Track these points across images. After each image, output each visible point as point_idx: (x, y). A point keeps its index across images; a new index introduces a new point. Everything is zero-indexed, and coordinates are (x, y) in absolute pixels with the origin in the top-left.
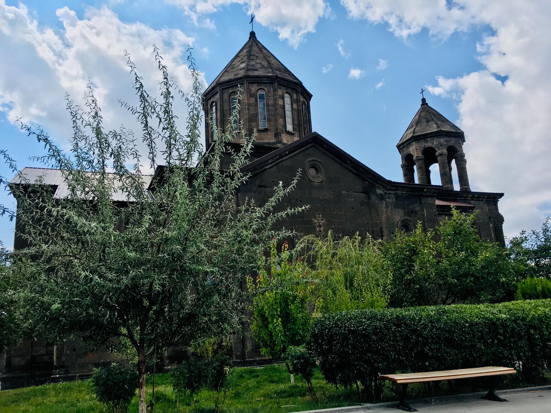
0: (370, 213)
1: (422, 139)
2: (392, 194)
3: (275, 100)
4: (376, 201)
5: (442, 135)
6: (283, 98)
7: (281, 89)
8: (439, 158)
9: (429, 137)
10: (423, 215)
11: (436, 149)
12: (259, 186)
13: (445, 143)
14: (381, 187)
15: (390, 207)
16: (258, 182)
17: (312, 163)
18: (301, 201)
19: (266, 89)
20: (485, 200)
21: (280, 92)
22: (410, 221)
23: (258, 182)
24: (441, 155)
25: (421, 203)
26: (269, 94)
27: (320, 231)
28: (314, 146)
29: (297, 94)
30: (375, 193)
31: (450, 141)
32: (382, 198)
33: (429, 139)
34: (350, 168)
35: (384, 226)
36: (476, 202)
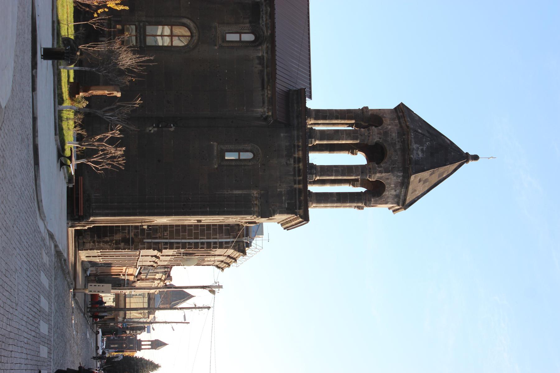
9: (400, 123)
13: (389, 139)
20: (297, 186)
31: (395, 151)
33: (397, 121)
36: (291, 169)
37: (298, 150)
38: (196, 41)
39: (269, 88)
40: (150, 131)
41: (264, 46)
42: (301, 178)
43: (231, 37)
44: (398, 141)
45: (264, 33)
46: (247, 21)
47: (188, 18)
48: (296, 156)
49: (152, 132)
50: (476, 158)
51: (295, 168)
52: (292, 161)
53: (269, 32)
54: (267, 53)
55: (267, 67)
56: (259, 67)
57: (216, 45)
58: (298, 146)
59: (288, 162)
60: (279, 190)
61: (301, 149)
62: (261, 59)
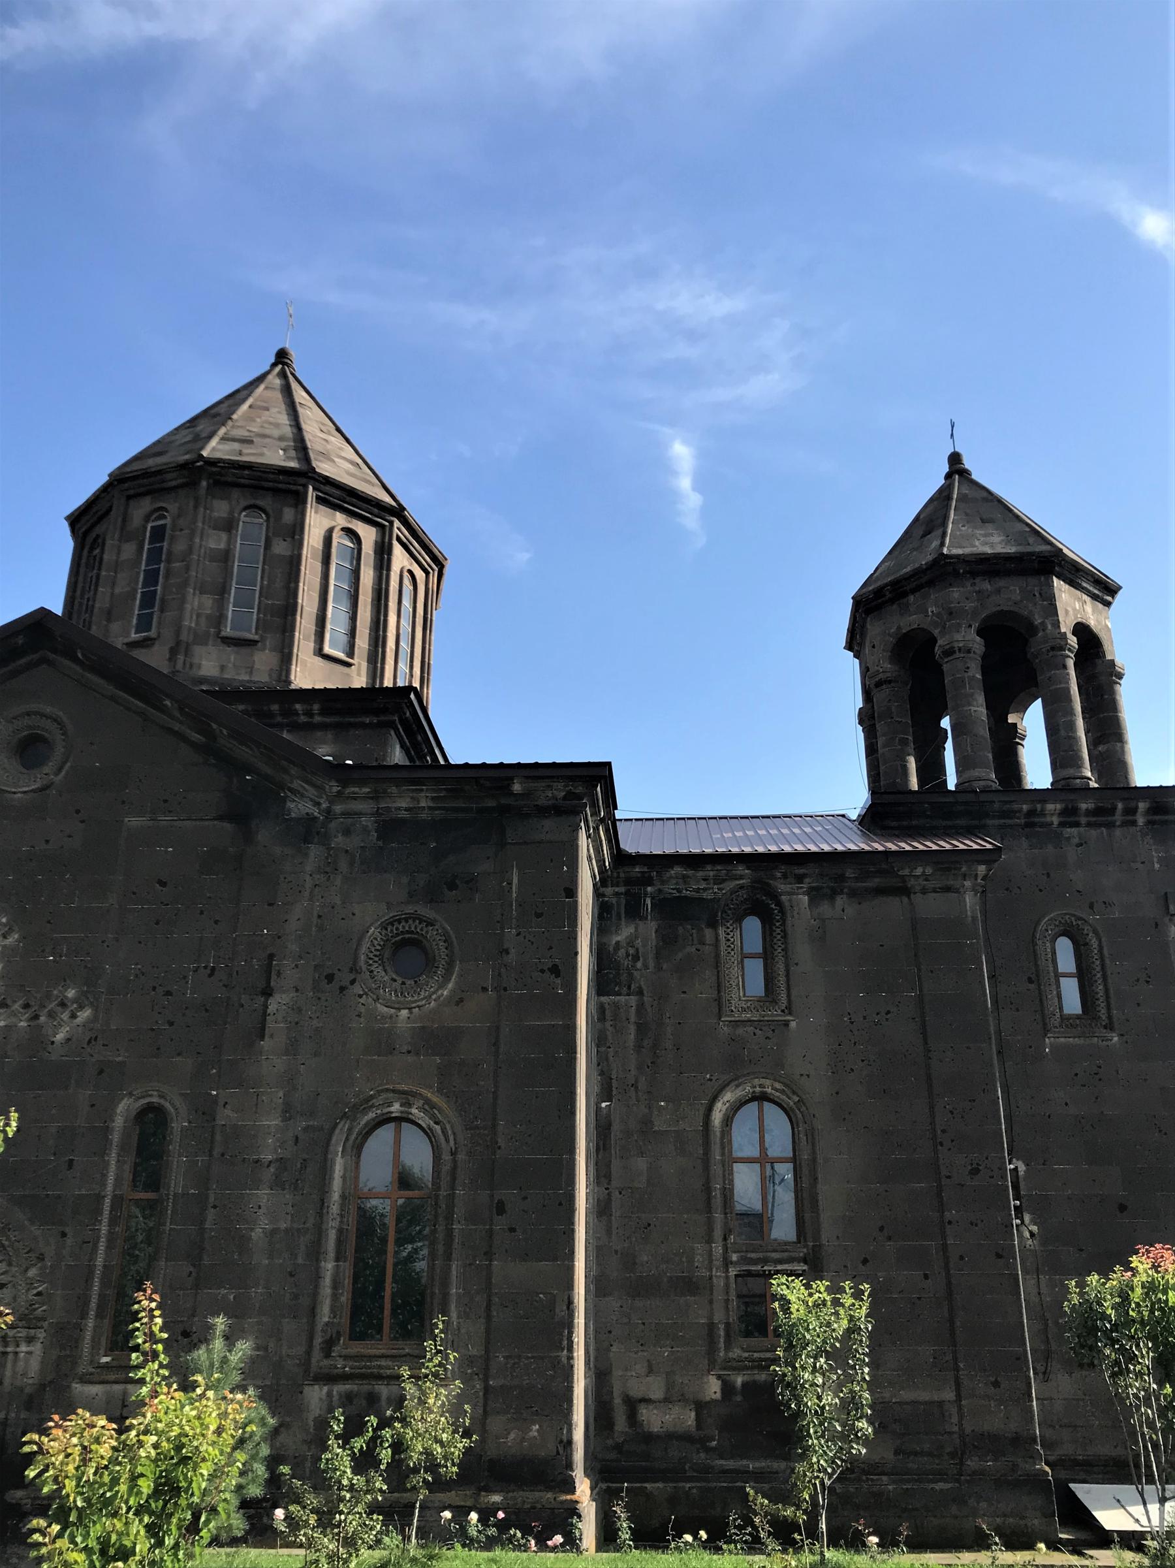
1: (892, 601)
2: (360, 814)
4: (278, 850)
5: (956, 574)
8: (945, 667)
9: (913, 591)
11: (936, 632)
13: (969, 605)
15: (343, 866)
17: (26, 721)
20: (1141, 821)
21: (221, 508)
22: (430, 923)
24: (949, 652)
31: (998, 591)
32: (307, 832)
33: (911, 598)
34: (177, 727)
35: (294, 947)
36: (1094, 833)
37: (1043, 814)
38: (778, 1085)
39: (906, 872)
40: (1032, 1234)
41: (782, 887)
42: (1120, 806)
43: (755, 983)
44: (974, 584)
45: (742, 887)
46: (708, 933)
47: (710, 1109)
48: (1056, 820)
49: (1035, 1228)
50: (955, 458)
51: (1089, 825)
52: (1068, 831)
53: (741, 870)
54: (800, 879)
55: (841, 878)
56: (840, 901)
57: (786, 1024)
58: (1031, 813)
59: (1076, 840)
60: (1157, 866)
61: (1039, 806)
62: (816, 895)
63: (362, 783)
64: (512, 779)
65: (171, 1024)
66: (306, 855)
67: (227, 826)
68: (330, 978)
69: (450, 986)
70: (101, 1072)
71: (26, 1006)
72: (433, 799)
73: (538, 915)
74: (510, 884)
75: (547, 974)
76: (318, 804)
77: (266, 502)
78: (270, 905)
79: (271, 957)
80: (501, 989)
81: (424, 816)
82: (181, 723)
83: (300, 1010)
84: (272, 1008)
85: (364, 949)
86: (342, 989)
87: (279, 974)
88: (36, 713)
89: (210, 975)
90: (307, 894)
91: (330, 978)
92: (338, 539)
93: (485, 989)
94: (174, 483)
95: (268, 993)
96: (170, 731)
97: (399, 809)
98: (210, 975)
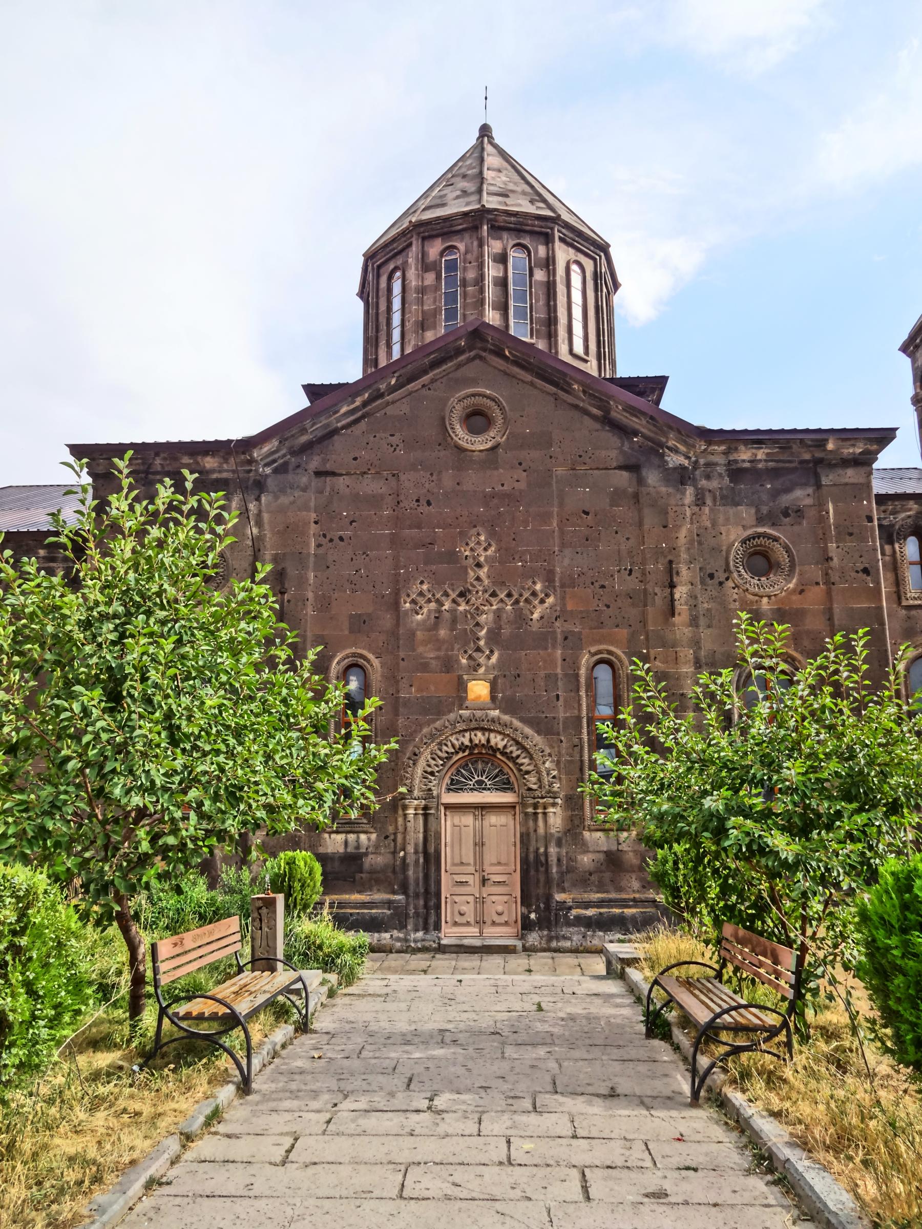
0: (640, 524)
3: (481, 266)
4: (663, 489)
6: (502, 259)
7: (500, 238)
10: (822, 520)
12: (318, 474)
14: (682, 448)
15: (709, 501)
16: (315, 463)
18: (429, 503)
19: (461, 246)
21: (496, 246)
23: (315, 463)
25: (818, 486)
26: (469, 256)
27: (478, 579)
28: (481, 358)
29: (547, 244)
30: (662, 464)
32: (682, 477)
35: (684, 556)
63: (719, 443)
64: (827, 440)
65: (608, 607)
66: (684, 493)
67: (625, 474)
68: (711, 576)
69: (794, 581)
70: (566, 638)
71: (509, 595)
72: (767, 454)
73: (851, 534)
74: (828, 513)
75: (861, 574)
76: (688, 458)
77: (526, 241)
78: (665, 527)
79: (671, 562)
80: (829, 583)
81: (760, 466)
82: (583, 401)
83: (696, 598)
84: (677, 596)
85: (732, 557)
86: (721, 584)
87: (678, 573)
88: (479, 395)
89: (630, 574)
90: (688, 520)
91: (711, 576)
92: (574, 267)
93: (817, 584)
94: (460, 227)
95: (672, 586)
96: (576, 407)
97: (744, 461)
98: (630, 574)
